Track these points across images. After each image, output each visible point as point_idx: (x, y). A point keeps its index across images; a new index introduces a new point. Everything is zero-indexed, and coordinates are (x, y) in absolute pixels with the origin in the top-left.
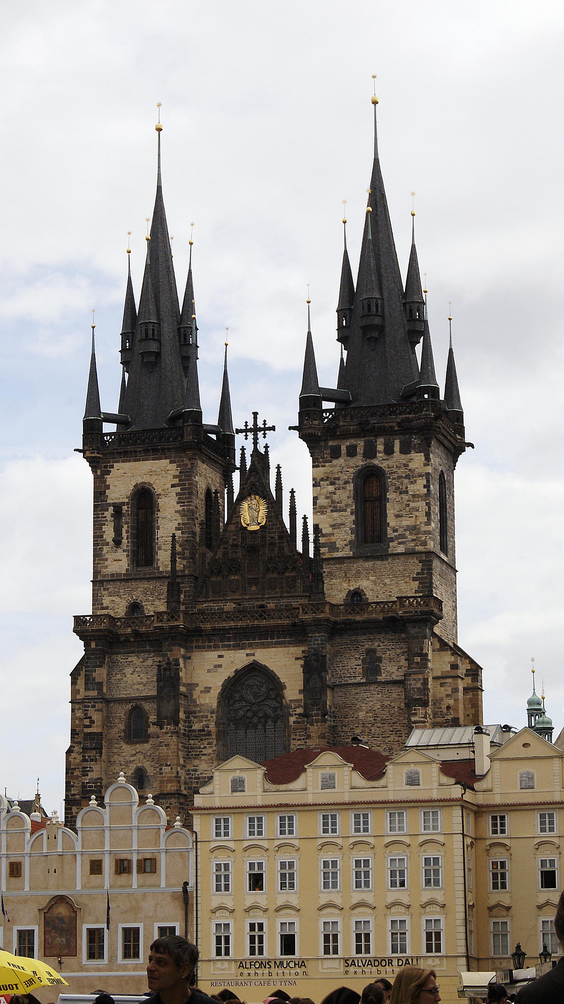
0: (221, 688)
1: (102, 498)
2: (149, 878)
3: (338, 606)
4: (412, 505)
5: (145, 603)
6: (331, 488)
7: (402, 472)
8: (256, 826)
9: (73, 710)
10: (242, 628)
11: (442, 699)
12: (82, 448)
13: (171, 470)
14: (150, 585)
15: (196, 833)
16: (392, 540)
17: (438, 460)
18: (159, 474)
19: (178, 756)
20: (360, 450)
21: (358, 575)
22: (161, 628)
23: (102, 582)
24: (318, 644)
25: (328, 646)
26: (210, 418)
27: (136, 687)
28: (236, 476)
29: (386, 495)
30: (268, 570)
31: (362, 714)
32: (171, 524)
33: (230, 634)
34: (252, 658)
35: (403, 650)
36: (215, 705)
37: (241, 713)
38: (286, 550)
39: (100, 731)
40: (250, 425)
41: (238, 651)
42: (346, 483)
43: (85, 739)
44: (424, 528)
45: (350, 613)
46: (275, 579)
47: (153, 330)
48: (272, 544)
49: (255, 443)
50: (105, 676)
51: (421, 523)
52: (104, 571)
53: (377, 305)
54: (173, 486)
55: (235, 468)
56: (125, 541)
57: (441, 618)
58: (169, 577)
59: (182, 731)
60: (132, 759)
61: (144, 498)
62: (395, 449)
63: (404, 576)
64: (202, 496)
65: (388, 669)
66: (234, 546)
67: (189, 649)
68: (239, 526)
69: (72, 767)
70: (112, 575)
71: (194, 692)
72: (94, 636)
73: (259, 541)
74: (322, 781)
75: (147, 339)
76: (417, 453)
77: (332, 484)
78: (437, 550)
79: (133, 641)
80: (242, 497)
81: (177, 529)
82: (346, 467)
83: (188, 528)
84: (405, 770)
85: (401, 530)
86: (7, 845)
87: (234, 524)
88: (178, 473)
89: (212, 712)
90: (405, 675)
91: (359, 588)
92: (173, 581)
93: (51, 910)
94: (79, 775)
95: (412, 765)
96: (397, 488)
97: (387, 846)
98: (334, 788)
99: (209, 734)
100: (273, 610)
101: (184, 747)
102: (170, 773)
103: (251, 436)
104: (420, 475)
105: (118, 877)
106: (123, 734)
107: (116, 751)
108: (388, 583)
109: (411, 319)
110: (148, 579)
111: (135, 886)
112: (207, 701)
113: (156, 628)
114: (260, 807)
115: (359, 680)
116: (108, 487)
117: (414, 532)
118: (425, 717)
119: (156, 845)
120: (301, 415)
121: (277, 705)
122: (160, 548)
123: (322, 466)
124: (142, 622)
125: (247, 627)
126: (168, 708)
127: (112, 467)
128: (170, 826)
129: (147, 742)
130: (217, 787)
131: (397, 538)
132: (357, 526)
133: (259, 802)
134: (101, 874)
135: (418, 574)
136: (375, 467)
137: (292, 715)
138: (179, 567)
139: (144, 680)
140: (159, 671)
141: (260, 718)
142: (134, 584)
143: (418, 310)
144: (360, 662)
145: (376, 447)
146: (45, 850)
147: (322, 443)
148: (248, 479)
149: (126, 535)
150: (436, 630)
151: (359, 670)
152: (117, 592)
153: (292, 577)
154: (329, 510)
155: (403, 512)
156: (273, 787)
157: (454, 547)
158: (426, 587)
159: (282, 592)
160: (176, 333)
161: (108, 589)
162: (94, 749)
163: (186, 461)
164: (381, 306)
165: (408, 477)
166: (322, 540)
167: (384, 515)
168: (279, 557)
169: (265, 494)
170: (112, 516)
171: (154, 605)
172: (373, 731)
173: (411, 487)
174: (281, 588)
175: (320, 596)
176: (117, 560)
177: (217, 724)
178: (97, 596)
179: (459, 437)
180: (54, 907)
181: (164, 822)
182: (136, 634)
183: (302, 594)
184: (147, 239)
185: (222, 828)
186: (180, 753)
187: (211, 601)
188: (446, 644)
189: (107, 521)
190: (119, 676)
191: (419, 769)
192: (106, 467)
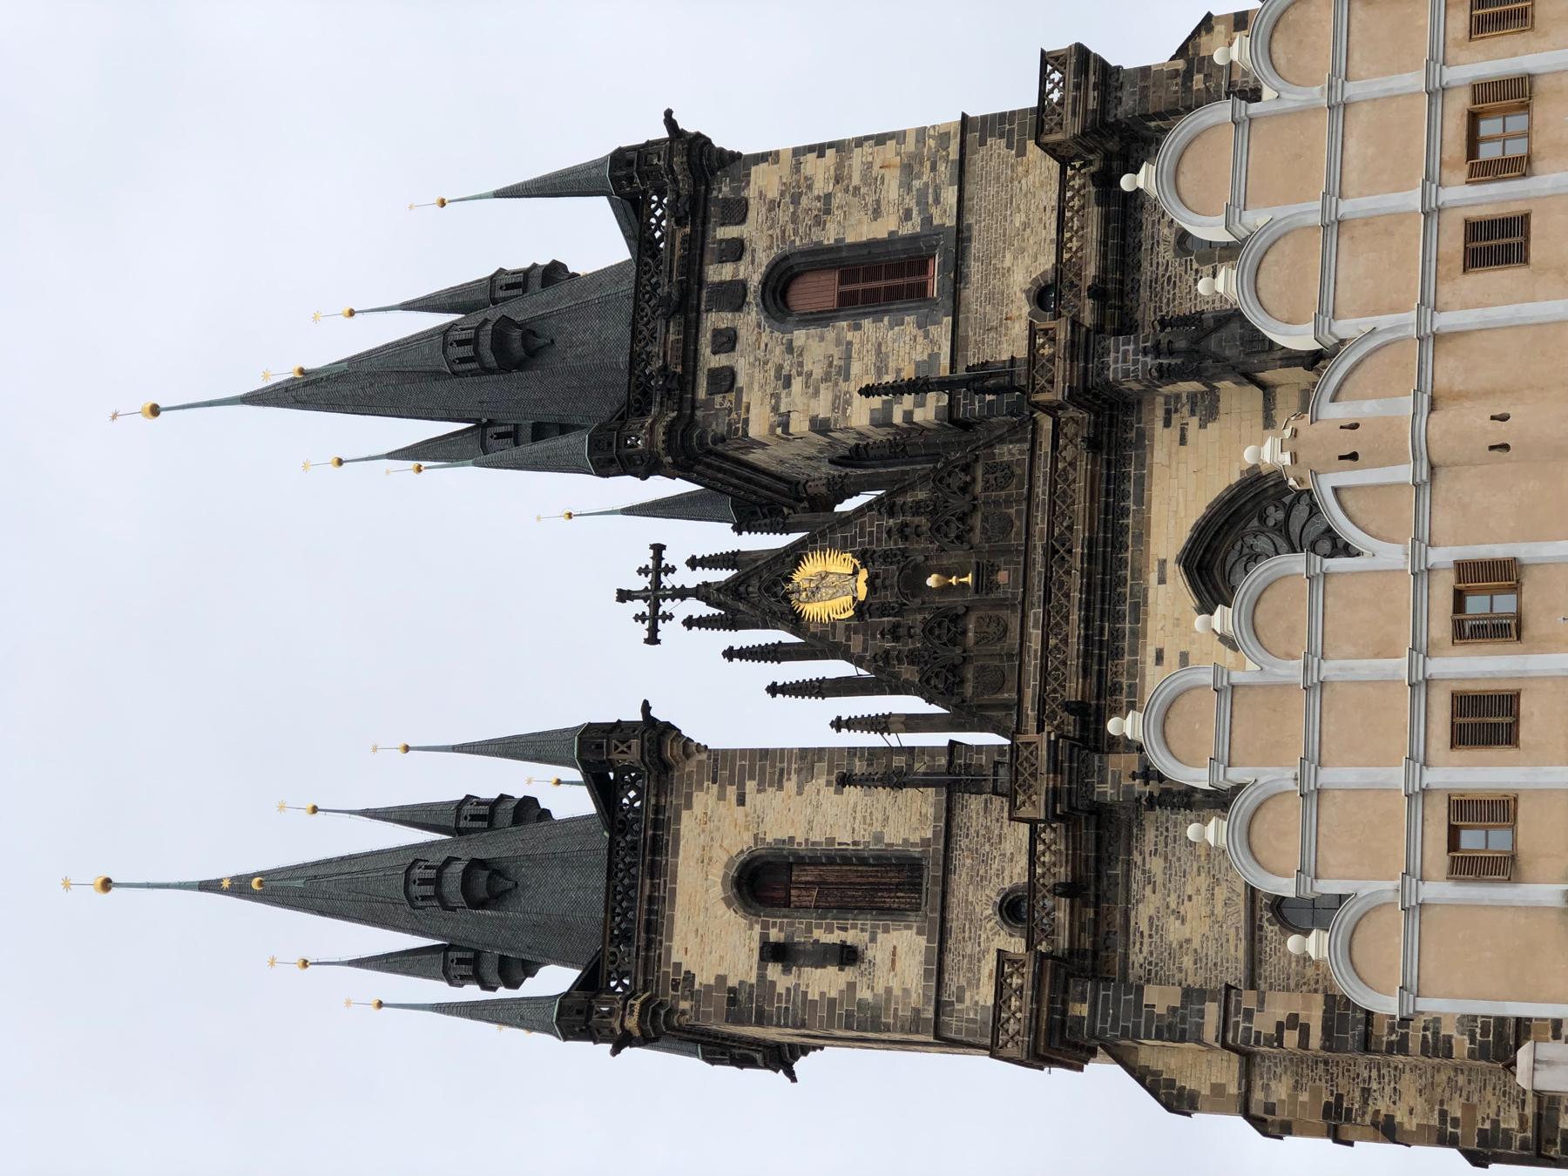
1: (742, 997)
4: (856, 181)
5: (1007, 879)
6: (797, 384)
7: (783, 216)
10: (1089, 588)
14: (963, 862)
16: (927, 220)
22: (1054, 795)
23: (939, 1006)
24: (1136, 353)
27: (1219, 910)
29: (829, 249)
32: (826, 806)
33: (1102, 629)
34: (1175, 573)
38: (921, 495)
40: (641, 607)
41: (1151, 608)
42: (790, 348)
46: (985, 519)
49: (681, 593)
51: (898, 154)
52: (915, 999)
54: (741, 801)
56: (851, 937)
61: (760, 881)
66: (896, 639)
69: (1435, 1121)
72: (1052, 1001)
76: (748, 183)
77: (788, 383)
79: (1096, 913)
80: (795, 622)
85: (907, 199)
86: (1377, 656)
87: (848, 639)
88: (716, 786)
91: (1027, 292)
94: (1462, 1100)
103: (666, 606)
104: (797, 168)
108: (1023, 218)
116: (721, 979)
122: (878, 838)
123: (748, 410)
125: (1088, 574)
127: (678, 966)
132: (886, 312)
134: (1525, 219)
135: (1009, 146)
136: (764, 283)
139: (1203, 881)
145: (722, 283)
147: (699, 414)
149: (837, 932)
152: (970, 962)
153: (986, 472)
154: (843, 386)
163: (691, 766)
165: (796, 200)
173: (820, 187)
174: (1008, 502)
176: (893, 961)
178: (974, 1021)
182: (1070, 890)
183: (1026, 446)
187: (1020, 692)
190: (1185, 959)
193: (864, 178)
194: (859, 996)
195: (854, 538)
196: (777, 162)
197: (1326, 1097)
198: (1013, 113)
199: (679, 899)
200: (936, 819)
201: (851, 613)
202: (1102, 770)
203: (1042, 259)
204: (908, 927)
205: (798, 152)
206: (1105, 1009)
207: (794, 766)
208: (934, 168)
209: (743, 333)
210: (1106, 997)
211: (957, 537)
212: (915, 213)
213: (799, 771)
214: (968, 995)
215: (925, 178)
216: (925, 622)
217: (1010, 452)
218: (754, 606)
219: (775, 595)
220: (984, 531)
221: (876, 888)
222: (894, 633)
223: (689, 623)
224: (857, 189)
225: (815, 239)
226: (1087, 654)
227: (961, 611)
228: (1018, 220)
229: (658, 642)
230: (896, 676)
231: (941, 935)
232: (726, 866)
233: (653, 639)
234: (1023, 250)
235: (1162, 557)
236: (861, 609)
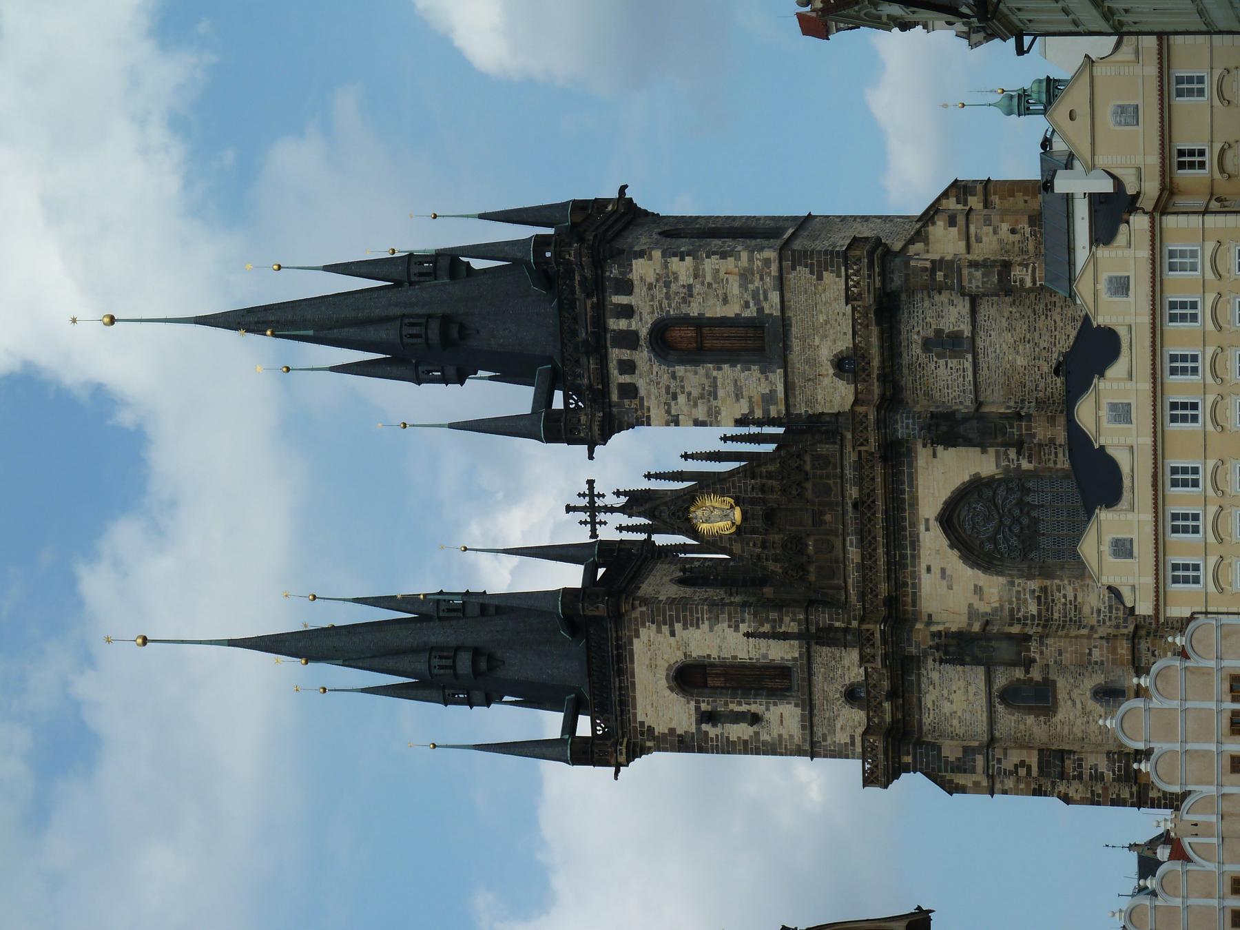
0: (976, 570)
1: (688, 739)
3: (856, 392)
4: (709, 279)
6: (682, 399)
7: (659, 293)
8: (1187, 523)
9: (1005, 792)
10: (887, 536)
11: (1000, 241)
15: (1193, 614)
16: (760, 310)
17: (643, 240)
18: (653, 652)
19: (1076, 637)
20: (626, 354)
21: (812, 362)
22: (885, 657)
23: (813, 744)
24: (914, 424)
25: (918, 408)
26: (571, 576)
27: (971, 697)
28: (660, 540)
29: (694, 318)
31: (1021, 361)
34: (934, 524)
35: (926, 298)
36: (1002, 580)
37: (1014, 541)
38: (772, 468)
39: (1035, 753)
40: (585, 516)
42: (674, 376)
43: (1048, 775)
45: (869, 375)
47: (441, 658)
48: (763, 489)
49: (612, 510)
50: (954, 743)
53: (412, 325)
54: (673, 634)
55: (648, 541)
56: (754, 708)
57: (879, 239)
58: (808, 644)
59: (1040, 629)
60: (1079, 706)
61: (689, 677)
62: (625, 302)
64: (688, 591)
65: (953, 320)
66: (764, 546)
67: (916, 617)
69: (1089, 795)
70: (803, 728)
71: (981, 611)
73: (758, 509)
74: (1120, 422)
75: (453, 667)
77: (675, 397)
78: (778, 243)
80: (692, 532)
81: (737, 629)
82: (650, 376)
83: (736, 613)
84: (1104, 297)
88: (654, 627)
89: (1012, 583)
90: (963, 295)
91: (831, 361)
92: (813, 637)
95: (1099, 287)
96: (684, 300)
97: (1220, 328)
98: (1129, 404)
99: (1044, 589)
100: (861, 490)
101: (1064, 627)
102: (1101, 649)
103: (601, 517)
104: (666, 265)
106: (1042, 718)
107: (1066, 730)
109: (433, 274)
110: (810, 674)
112: (995, 591)
113: (884, 665)
114: (1156, 517)
115: (968, 365)
116: (672, 731)
118: (1026, 266)
119: (1209, 674)
120: (571, 441)
121: (1002, 488)
122: (765, 656)
124: (875, 686)
125: (886, 528)
126: (1005, 650)
127: (642, 723)
128: (1183, 654)
129: (1054, 682)
130: (1124, 580)
131: (758, 302)
132: (739, 362)
133: (1148, 517)
135: (812, 273)
137: (1019, 466)
138: (793, 627)
139: (962, 684)
140: (947, 662)
141: (1021, 511)
142: (817, 696)
143: (421, 264)
144: (942, 362)
145: (621, 331)
146: (1214, 840)
147: (615, 410)
148: (665, 522)
150: (897, 246)
151: (953, 363)
154: (714, 403)
155: (720, 292)
156: (1126, 495)
157: (773, 218)
158: (832, 261)
159: (835, 476)
162: (1063, 761)
163: (636, 614)
164: (412, 320)
165: (667, 285)
166: (758, 414)
167: (723, 322)
168: (782, 479)
169: (689, 498)
170: (714, 725)
171: (848, 666)
172: (1045, 345)
173: (685, 278)
174: (828, 477)
175: (841, 419)
177: (1030, 577)
179: (610, 208)
181: (1177, 663)
182: (892, 695)
183: (837, 447)
185: (1187, 574)
186: (1073, 633)
187: (845, 582)
188: (918, 232)
189: (722, 734)
191: (1104, 276)
192: (642, 734)
197: (1033, 786)
202: (909, 640)
203: (839, 343)
209: (639, 363)
213: (709, 619)
217: (824, 449)
224: (710, 284)
226: (889, 570)
228: (822, 318)
231: (809, 708)
234: (826, 337)
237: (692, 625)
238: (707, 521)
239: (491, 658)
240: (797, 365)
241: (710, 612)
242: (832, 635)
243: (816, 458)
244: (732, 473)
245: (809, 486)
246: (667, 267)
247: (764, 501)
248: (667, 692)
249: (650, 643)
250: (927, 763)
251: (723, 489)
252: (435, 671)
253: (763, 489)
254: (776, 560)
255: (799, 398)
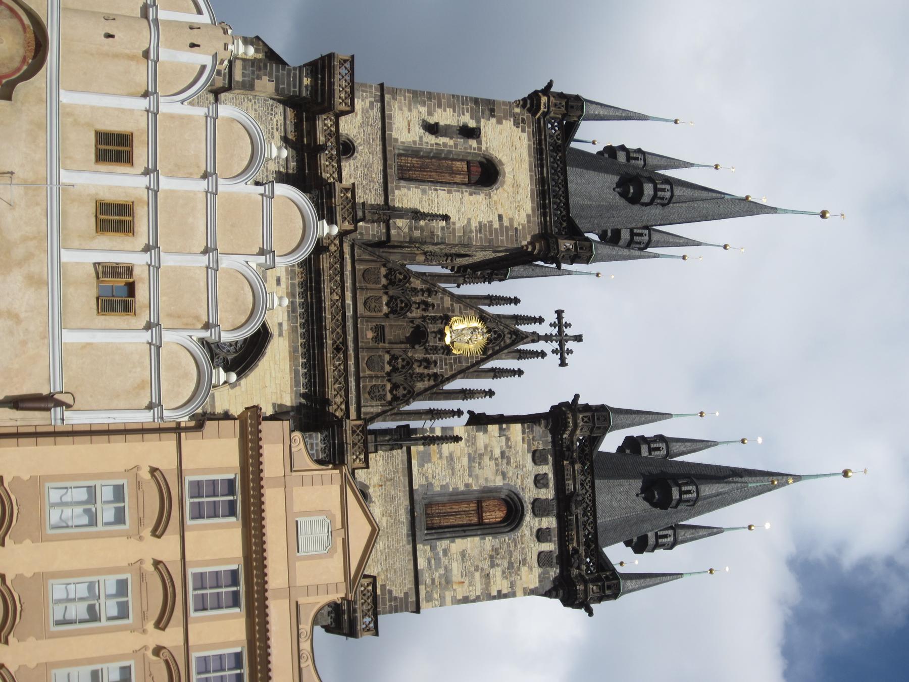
1: (487, 112)
2: (85, 296)
6: (497, 453)
7: (517, 555)
10: (320, 319)
12: (552, 90)
13: (519, 215)
16: (433, 548)
21: (390, 499)
22: (330, 194)
30: (394, 358)
38: (420, 386)
40: (568, 331)
42: (504, 475)
44: (448, 595)
46: (383, 368)
48: (427, 363)
49: (547, 338)
51: (455, 590)
54: (500, 217)
56: (431, 139)
61: (486, 174)
63: (387, 570)
68: (450, 314)
70: (390, 117)
72: (323, 84)
75: (656, 190)
76: (539, 576)
87: (452, 305)
88: (515, 225)
91: (372, 501)
92: (386, 212)
93: (7, 12)
104: (512, 585)
105: (91, 209)
111: (67, 256)
116: (499, 122)
117: (443, 580)
120: (586, 407)
123: (523, 439)
127: (523, 131)
132: (451, 494)
135: (390, 592)
138: (400, 223)
145: (547, 515)
147: (550, 439)
152: (368, 122)
153: (385, 395)
154: (470, 450)
155: (468, 563)
160: (644, 224)
161: (372, 108)
173: (497, 573)
174: (371, 377)
176: (409, 125)
178: (363, 91)
180: (15, 22)
183: (363, 410)
184: (747, 197)
189: (459, 116)
193: (473, 577)
194: (426, 109)
195: (455, 363)
196: (524, 589)
198: (390, 612)
199: (526, 166)
200: (393, 200)
201: (453, 319)
204: (403, 143)
205: (513, 594)
206: (294, 81)
207: (474, 234)
208: (433, 580)
209: (532, 485)
210: (295, 87)
211: (397, 358)
212: (441, 553)
213: (471, 231)
214: (368, 105)
215: (438, 575)
216: (410, 310)
218: (507, 326)
219: (495, 332)
220: (383, 361)
221: (422, 168)
222: (426, 306)
223: (540, 320)
224: (476, 570)
225: (497, 540)
227: (391, 316)
229: (556, 312)
230: (424, 282)
232: (504, 182)
233: (559, 313)
235: (281, 339)
236: (446, 320)
237: (485, 225)
238: (475, 329)
239: (624, 195)
240: (401, 494)
241: (470, 238)
242: (376, 217)
243: (383, 397)
244: (453, 377)
245: (388, 368)
246: (511, 583)
247: (427, 351)
248: (504, 159)
249: (518, 208)
250: (289, 74)
251: (460, 362)
252: (668, 187)
253: (427, 363)
254: (415, 291)
255: (399, 461)
